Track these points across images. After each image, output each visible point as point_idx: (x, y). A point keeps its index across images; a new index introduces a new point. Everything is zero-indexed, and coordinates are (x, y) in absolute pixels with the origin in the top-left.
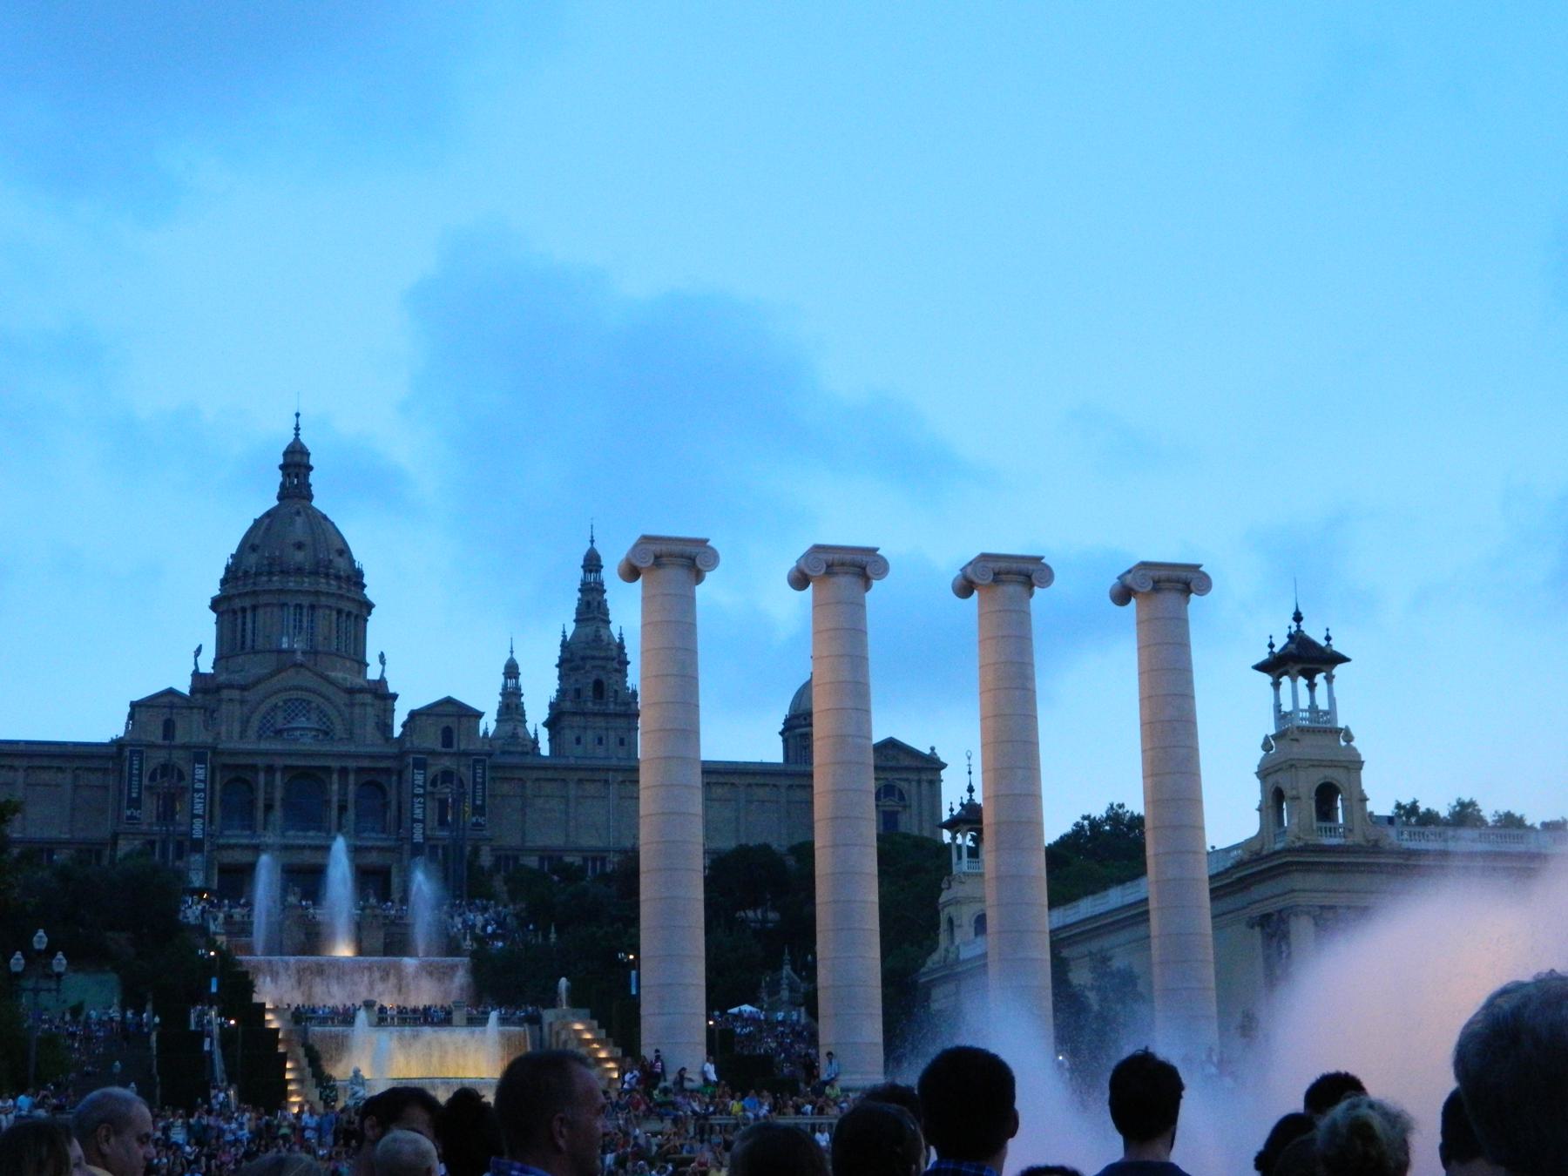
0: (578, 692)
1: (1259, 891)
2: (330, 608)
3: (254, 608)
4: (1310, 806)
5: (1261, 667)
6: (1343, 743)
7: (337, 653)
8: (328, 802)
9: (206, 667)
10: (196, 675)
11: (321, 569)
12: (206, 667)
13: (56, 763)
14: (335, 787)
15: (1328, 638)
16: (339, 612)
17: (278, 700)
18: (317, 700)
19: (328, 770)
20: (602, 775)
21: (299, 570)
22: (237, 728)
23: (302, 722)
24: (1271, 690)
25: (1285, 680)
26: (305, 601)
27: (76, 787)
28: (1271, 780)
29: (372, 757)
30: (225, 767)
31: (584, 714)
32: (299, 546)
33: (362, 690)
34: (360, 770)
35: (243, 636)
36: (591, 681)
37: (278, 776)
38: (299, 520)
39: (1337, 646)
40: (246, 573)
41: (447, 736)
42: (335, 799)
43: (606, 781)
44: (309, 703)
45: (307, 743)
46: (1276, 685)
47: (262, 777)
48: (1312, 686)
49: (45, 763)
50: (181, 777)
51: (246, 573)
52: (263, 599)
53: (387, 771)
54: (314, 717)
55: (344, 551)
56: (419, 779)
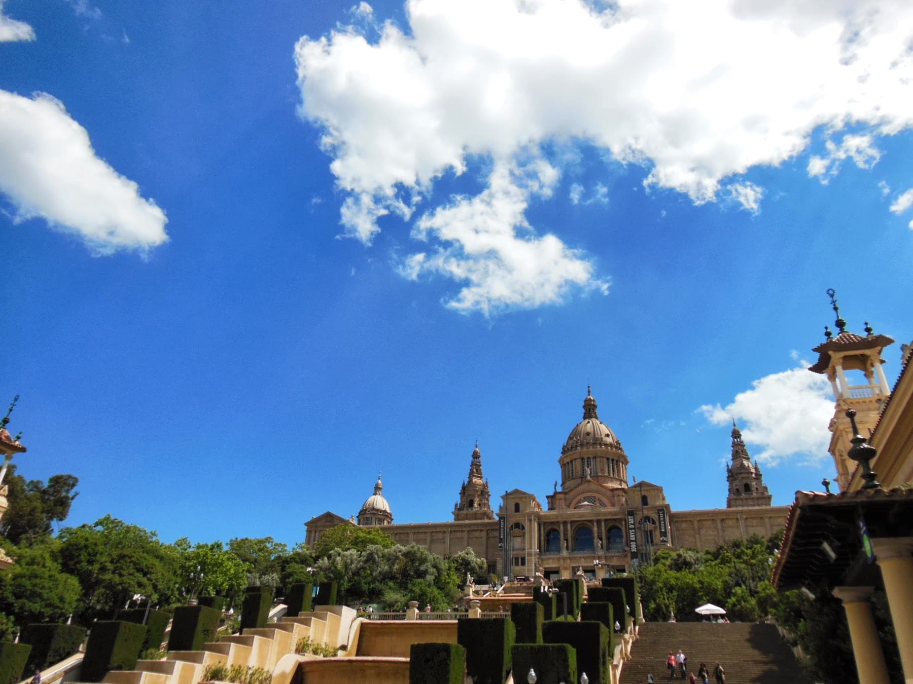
3: (571, 461)
7: (608, 477)
9: (559, 489)
14: (595, 529)
16: (608, 459)
17: (581, 497)
18: (598, 496)
27: (488, 538)
30: (545, 523)
32: (588, 434)
34: (606, 520)
37: (569, 526)
41: (645, 500)
42: (596, 535)
43: (737, 519)
50: (523, 528)
53: (620, 520)
56: (631, 520)
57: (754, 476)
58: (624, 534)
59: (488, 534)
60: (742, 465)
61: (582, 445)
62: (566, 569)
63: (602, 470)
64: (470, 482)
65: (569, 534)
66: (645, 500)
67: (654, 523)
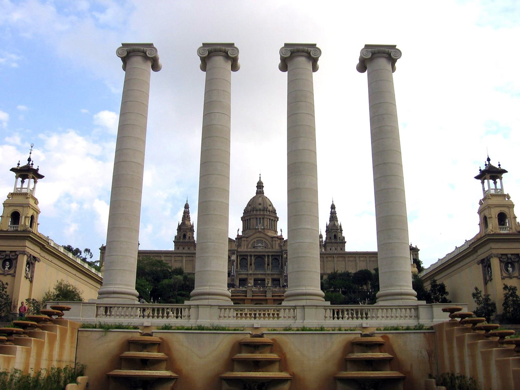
0: (330, 238)
1: (480, 252)
3: (250, 219)
4: (496, 221)
5: (477, 178)
6: (507, 199)
7: (269, 229)
8: (265, 263)
9: (240, 234)
10: (238, 235)
11: (265, 209)
12: (240, 234)
15: (499, 165)
16: (270, 219)
17: (255, 240)
18: (264, 240)
19: (264, 255)
20: (332, 256)
21: (260, 210)
22: (246, 247)
23: (260, 245)
24: (481, 185)
25: (486, 181)
26: (261, 217)
28: (482, 214)
29: (274, 252)
31: (332, 243)
32: (260, 204)
34: (272, 255)
38: (260, 198)
39: (502, 167)
40: (248, 211)
45: (259, 249)
46: (483, 183)
48: (495, 183)
51: (248, 211)
52: (252, 217)
53: (279, 255)
54: (264, 244)
55: (271, 205)
58: (281, 263)
60: (335, 224)
61: (257, 210)
62: (251, 279)
63: (267, 226)
64: (183, 223)
65: (253, 262)
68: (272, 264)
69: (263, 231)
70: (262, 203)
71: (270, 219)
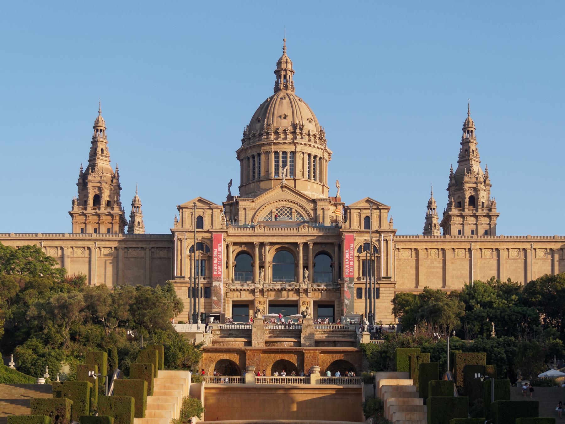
2: (303, 153)
3: (259, 155)
8: (297, 265)
12: (236, 192)
13: (140, 245)
14: (301, 255)
16: (309, 155)
17: (273, 207)
18: (295, 207)
19: (296, 245)
33: (322, 200)
35: (254, 173)
36: (467, 197)
37: (267, 248)
40: (254, 134)
41: (368, 222)
42: (301, 262)
43: (470, 250)
44: (291, 209)
47: (257, 250)
49: (134, 245)
52: (264, 149)
57: (482, 186)
59: (152, 253)
61: (276, 133)
66: (368, 222)
67: (377, 250)
68: (314, 266)
69: (291, 184)
70: (289, 113)
71: (309, 155)
